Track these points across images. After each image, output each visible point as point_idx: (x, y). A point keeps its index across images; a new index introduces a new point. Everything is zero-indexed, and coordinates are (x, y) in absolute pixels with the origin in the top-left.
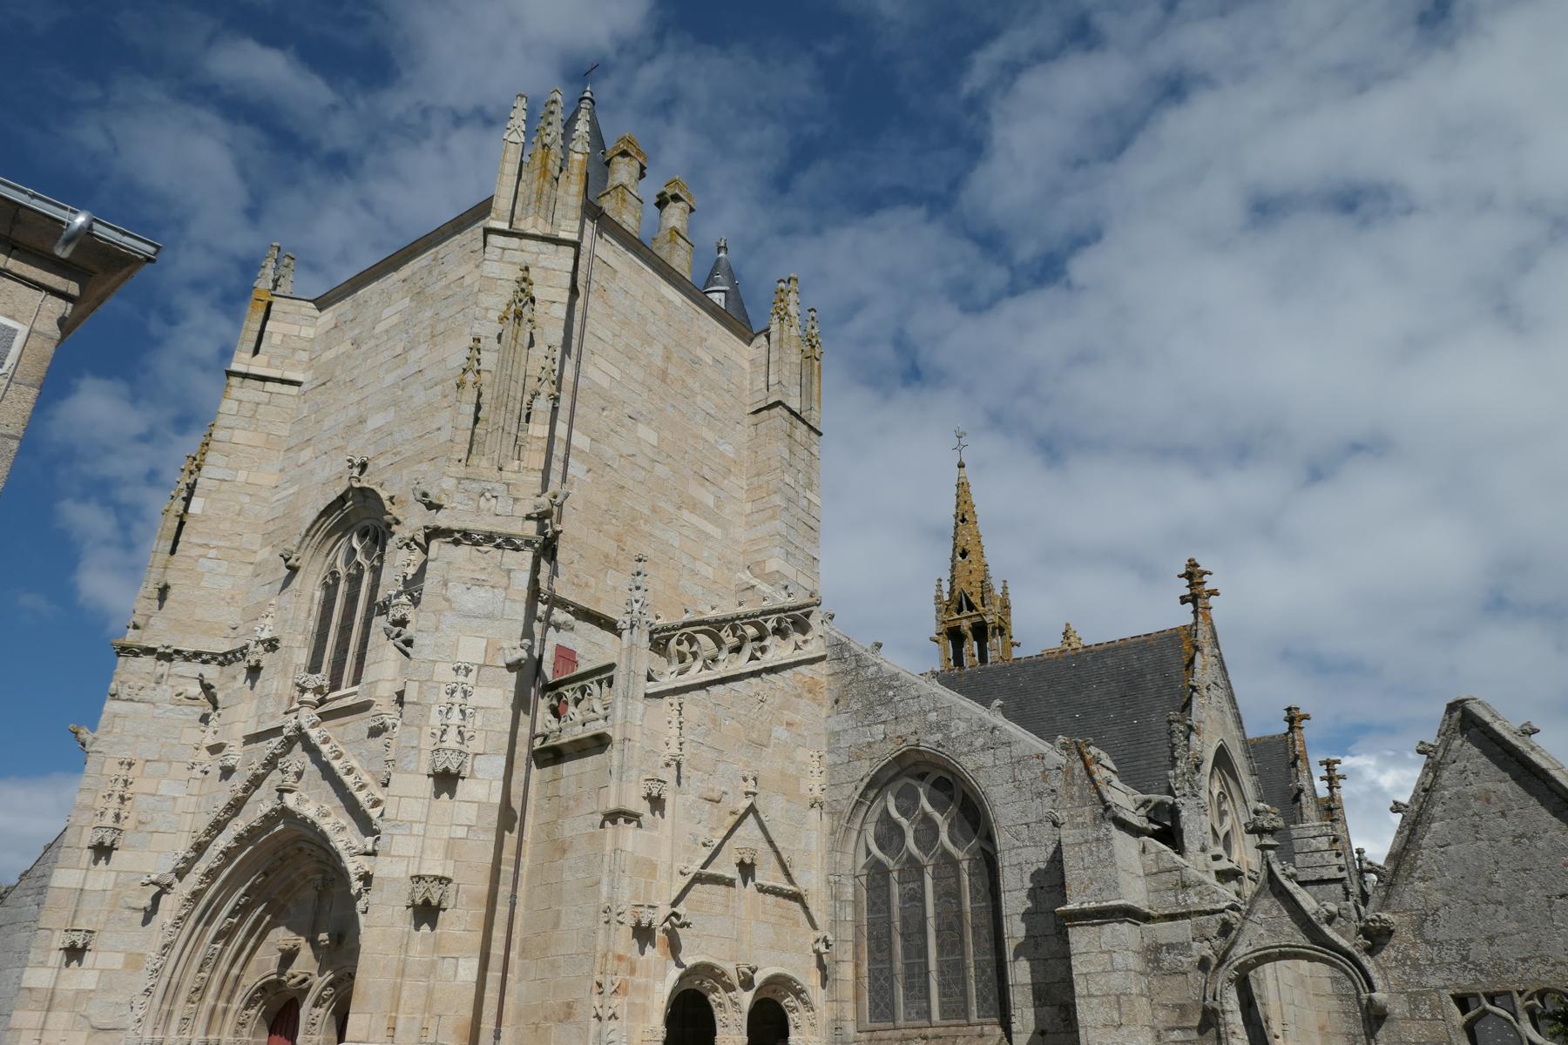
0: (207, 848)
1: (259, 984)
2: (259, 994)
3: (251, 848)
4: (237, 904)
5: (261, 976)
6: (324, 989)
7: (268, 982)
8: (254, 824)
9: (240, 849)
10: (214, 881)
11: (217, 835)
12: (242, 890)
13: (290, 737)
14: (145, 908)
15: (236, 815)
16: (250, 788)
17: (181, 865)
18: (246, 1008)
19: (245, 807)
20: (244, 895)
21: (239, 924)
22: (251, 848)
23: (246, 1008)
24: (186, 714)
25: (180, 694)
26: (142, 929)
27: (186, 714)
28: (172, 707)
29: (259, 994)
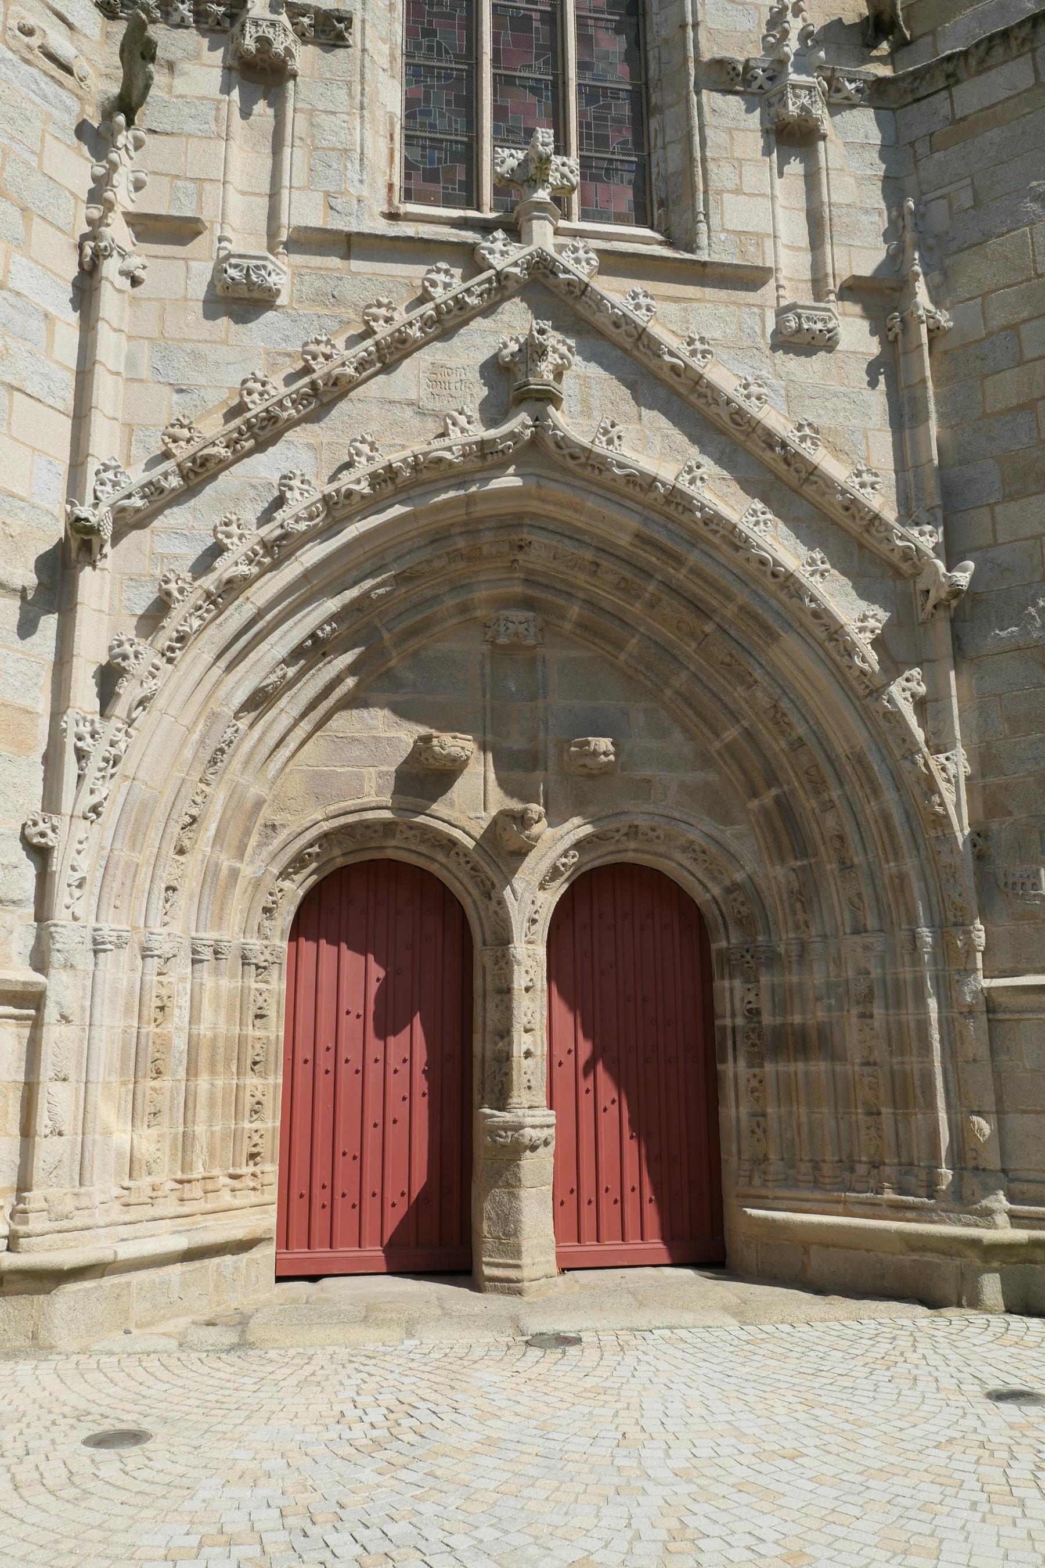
0: (214, 477)
1: (326, 826)
2: (316, 849)
3: (398, 510)
4: (313, 636)
5: (333, 809)
6: (565, 855)
7: (365, 825)
8: (448, 455)
9: (371, 505)
10: (275, 566)
11: (250, 453)
12: (332, 605)
13: (507, 276)
14: (24, 589)
15: (313, 418)
16: (372, 363)
17: (137, 502)
18: (284, 875)
19: (343, 406)
20: (334, 618)
21: (291, 684)
22: (398, 510)
23: (284, 875)
24: (45, 98)
25: (29, 32)
26: (19, 644)
27: (45, 98)
28: (10, 55)
29: (316, 849)
